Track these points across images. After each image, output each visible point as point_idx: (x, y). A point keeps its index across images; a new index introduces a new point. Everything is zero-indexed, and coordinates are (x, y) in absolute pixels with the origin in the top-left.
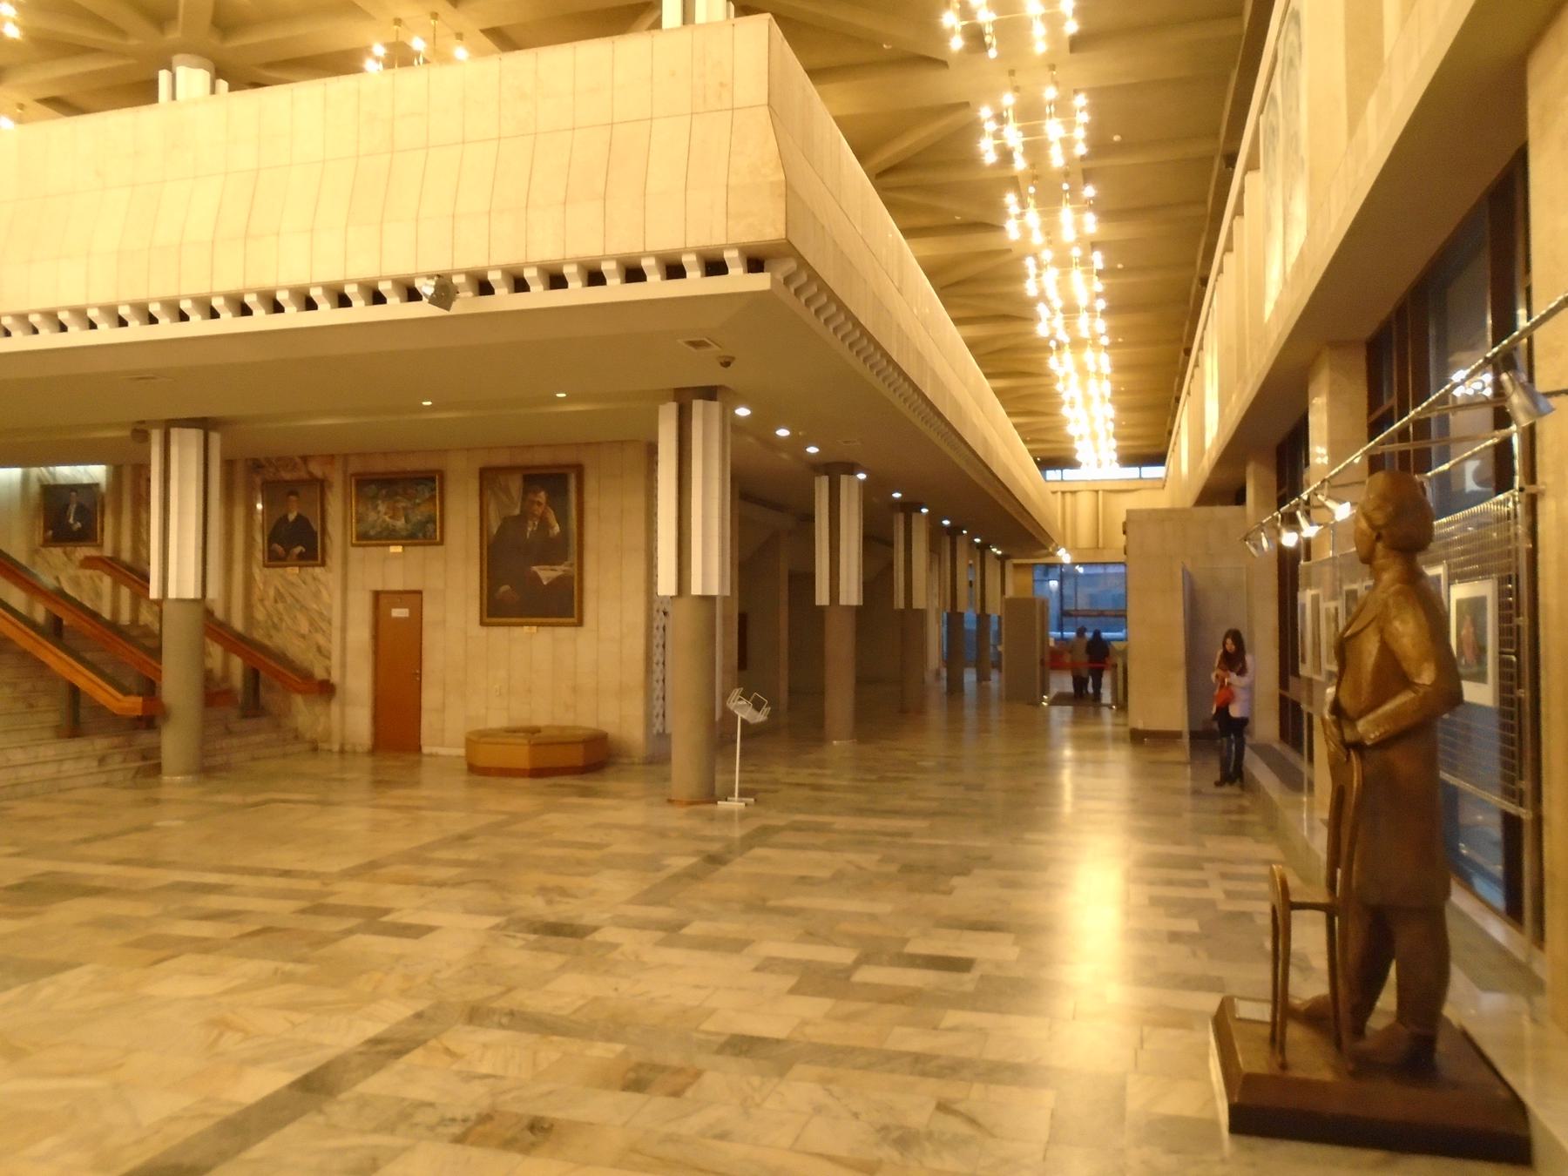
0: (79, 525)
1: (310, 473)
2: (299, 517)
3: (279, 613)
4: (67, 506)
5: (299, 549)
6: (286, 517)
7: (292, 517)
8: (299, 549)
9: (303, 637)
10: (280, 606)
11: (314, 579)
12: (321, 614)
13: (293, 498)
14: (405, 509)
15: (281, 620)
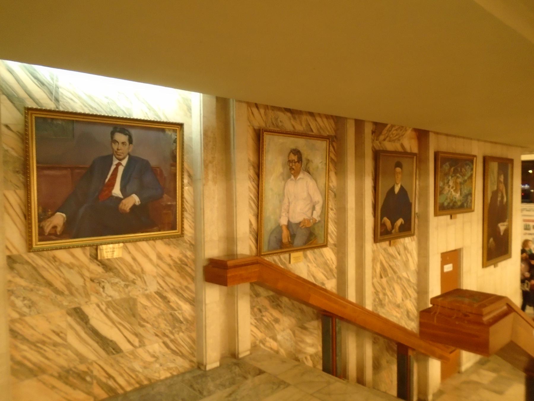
0: (135, 199)
1: (402, 146)
2: (402, 189)
3: (384, 289)
4: (107, 161)
5: (400, 221)
6: (393, 188)
7: (397, 189)
8: (400, 221)
9: (398, 306)
10: (384, 280)
11: (405, 248)
12: (408, 281)
13: (398, 169)
14: (461, 183)
15: (385, 294)
